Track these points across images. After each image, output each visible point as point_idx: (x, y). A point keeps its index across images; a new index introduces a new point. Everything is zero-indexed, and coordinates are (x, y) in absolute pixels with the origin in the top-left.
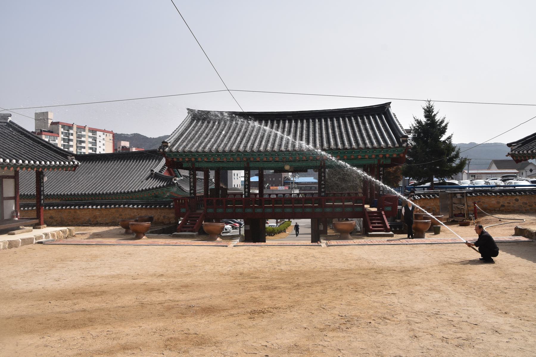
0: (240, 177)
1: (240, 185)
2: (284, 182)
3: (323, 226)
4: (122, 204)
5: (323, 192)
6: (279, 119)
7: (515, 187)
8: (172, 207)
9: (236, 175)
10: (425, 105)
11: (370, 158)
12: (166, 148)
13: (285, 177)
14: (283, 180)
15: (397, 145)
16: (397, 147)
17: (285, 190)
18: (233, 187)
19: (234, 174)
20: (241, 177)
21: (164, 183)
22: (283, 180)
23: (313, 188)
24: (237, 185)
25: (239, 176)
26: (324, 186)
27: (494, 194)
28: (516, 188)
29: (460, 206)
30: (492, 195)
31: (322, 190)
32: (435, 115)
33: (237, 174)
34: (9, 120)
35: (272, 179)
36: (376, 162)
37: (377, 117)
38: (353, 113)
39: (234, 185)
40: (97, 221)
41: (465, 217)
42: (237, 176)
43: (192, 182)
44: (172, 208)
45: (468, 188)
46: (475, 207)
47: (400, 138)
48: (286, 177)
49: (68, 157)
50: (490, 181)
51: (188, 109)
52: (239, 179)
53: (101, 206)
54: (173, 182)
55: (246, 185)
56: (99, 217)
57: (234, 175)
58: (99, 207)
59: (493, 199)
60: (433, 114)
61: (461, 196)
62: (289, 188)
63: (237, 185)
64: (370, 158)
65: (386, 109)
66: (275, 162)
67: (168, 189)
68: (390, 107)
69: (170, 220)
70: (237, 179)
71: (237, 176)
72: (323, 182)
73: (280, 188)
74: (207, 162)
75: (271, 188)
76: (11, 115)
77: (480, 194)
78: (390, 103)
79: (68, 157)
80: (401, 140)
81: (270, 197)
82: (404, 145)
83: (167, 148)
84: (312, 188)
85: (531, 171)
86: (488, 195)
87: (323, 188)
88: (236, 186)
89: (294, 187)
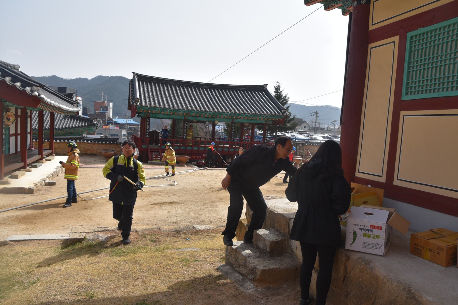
2: (107, 122)
3: (231, 160)
4: (77, 139)
5: (232, 139)
6: (198, 87)
7: (308, 141)
8: (119, 143)
10: (276, 85)
11: (260, 119)
12: (137, 103)
14: (106, 120)
15: (281, 114)
16: (281, 115)
17: (116, 130)
21: (82, 123)
22: (106, 120)
23: (133, 129)
26: (233, 135)
27: (317, 145)
28: (317, 141)
29: (301, 151)
30: (316, 145)
31: (232, 137)
32: (281, 92)
34: (19, 71)
36: (264, 122)
37: (260, 92)
38: (245, 88)
40: (56, 152)
41: (303, 157)
43: (148, 127)
44: (115, 144)
45: (295, 140)
46: (308, 152)
47: (282, 110)
49: (74, 104)
50: (295, 135)
51: (133, 73)
53: (60, 140)
54: (94, 123)
55: (185, 131)
56: (58, 149)
58: (58, 141)
59: (316, 148)
60: (280, 91)
61: (302, 145)
64: (260, 119)
65: (265, 88)
66: (204, 117)
67: (88, 128)
68: (267, 87)
69: (117, 153)
72: (233, 133)
74: (159, 114)
76: (19, 66)
77: (310, 144)
78: (267, 85)
79: (74, 104)
80: (283, 111)
81: (200, 140)
82: (285, 114)
83: (138, 103)
84: (132, 128)
85: (305, 127)
86: (314, 145)
87: (233, 136)
89: (127, 128)
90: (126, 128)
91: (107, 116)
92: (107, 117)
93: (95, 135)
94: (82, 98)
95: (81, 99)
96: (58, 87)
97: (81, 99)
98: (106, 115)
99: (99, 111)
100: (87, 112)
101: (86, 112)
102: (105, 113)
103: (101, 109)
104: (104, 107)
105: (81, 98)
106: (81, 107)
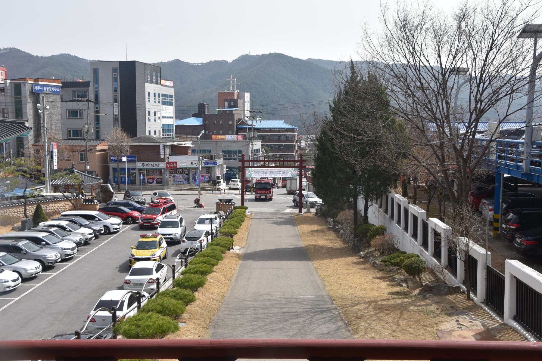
0: (159, 118)
1: (160, 131)
2: (237, 128)
9: (152, 114)
13: (239, 120)
14: (235, 123)
18: (147, 134)
19: (149, 112)
20: (163, 117)
22: (235, 123)
23: (283, 138)
24: (155, 132)
25: (158, 115)
33: (155, 113)
35: (218, 123)
39: (150, 132)
42: (155, 115)
48: (241, 120)
52: (158, 120)
57: (149, 114)
62: (245, 137)
63: (155, 132)
70: (155, 120)
71: (155, 115)
73: (227, 137)
75: (214, 137)
88: (152, 134)
89: (254, 137)
90: (251, 136)
91: (235, 116)
92: (236, 118)
93: (185, 153)
94: (174, 83)
95: (172, 85)
96: (121, 63)
97: (172, 85)
98: (234, 114)
99: (222, 108)
100: (204, 112)
101: (202, 110)
102: (233, 110)
103: (226, 104)
104: (231, 100)
105: (172, 82)
106: (172, 100)
